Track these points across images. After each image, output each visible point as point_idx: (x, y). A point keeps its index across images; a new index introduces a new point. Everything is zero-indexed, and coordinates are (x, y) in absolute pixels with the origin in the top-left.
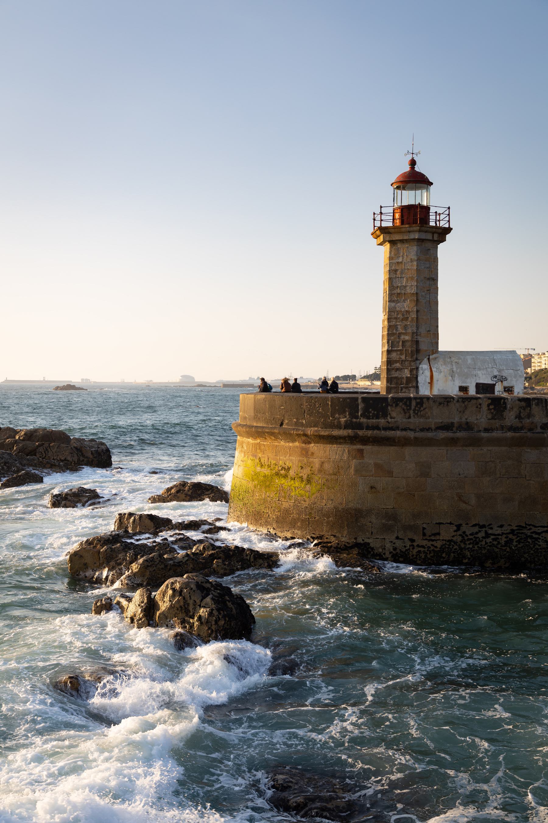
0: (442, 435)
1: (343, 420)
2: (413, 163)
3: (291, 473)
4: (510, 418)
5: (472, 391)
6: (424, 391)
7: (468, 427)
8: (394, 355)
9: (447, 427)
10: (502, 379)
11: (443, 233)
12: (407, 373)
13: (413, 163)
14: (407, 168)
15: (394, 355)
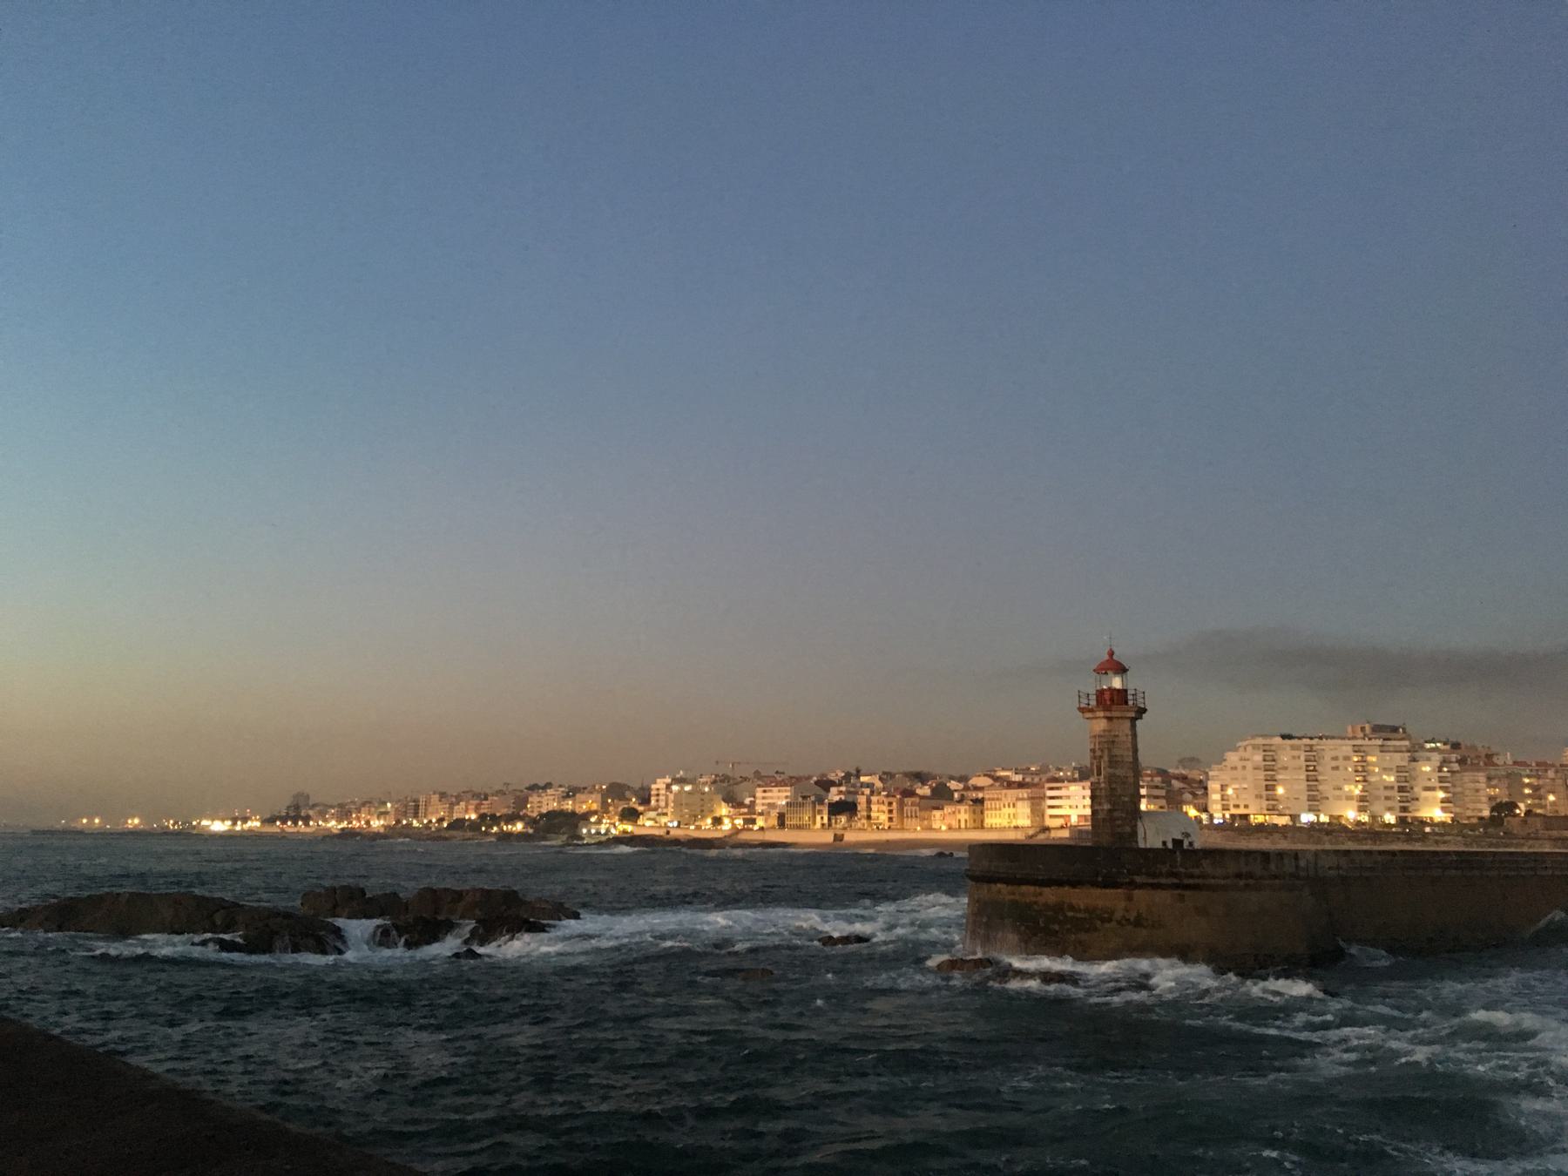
0: (1242, 883)
1: (1164, 870)
2: (1111, 654)
3: (1118, 915)
4: (1273, 866)
5: (1170, 846)
6: (1142, 845)
7: (1250, 876)
8: (1116, 814)
9: (1239, 876)
10: (1187, 835)
11: (1142, 711)
12: (1128, 829)
13: (1111, 654)
14: (1106, 657)
15: (1116, 814)
